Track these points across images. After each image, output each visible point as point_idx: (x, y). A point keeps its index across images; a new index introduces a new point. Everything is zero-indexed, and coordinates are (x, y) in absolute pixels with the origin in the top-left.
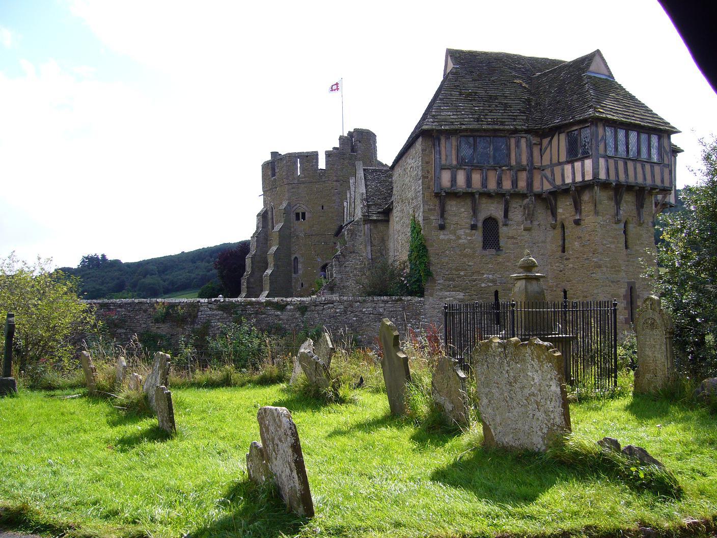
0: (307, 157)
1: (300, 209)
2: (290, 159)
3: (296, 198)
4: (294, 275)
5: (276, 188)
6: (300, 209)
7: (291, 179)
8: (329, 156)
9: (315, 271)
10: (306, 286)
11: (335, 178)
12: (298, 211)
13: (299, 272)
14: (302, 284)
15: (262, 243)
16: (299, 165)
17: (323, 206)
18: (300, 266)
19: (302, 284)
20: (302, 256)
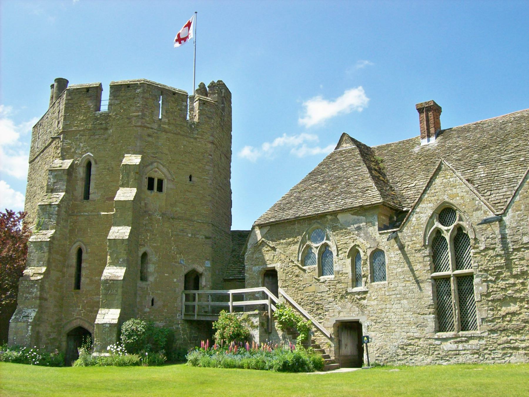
0: (174, 93)
1: (156, 172)
2: (149, 89)
3: (153, 153)
4: (140, 284)
5: (106, 129)
6: (156, 172)
7: (148, 119)
8: (204, 104)
9: (175, 280)
10: (159, 303)
11: (211, 138)
12: (152, 176)
13: (151, 279)
14: (153, 300)
15: (63, 219)
16: (161, 102)
17: (190, 177)
18: (151, 268)
19: (153, 300)
20: (156, 252)
